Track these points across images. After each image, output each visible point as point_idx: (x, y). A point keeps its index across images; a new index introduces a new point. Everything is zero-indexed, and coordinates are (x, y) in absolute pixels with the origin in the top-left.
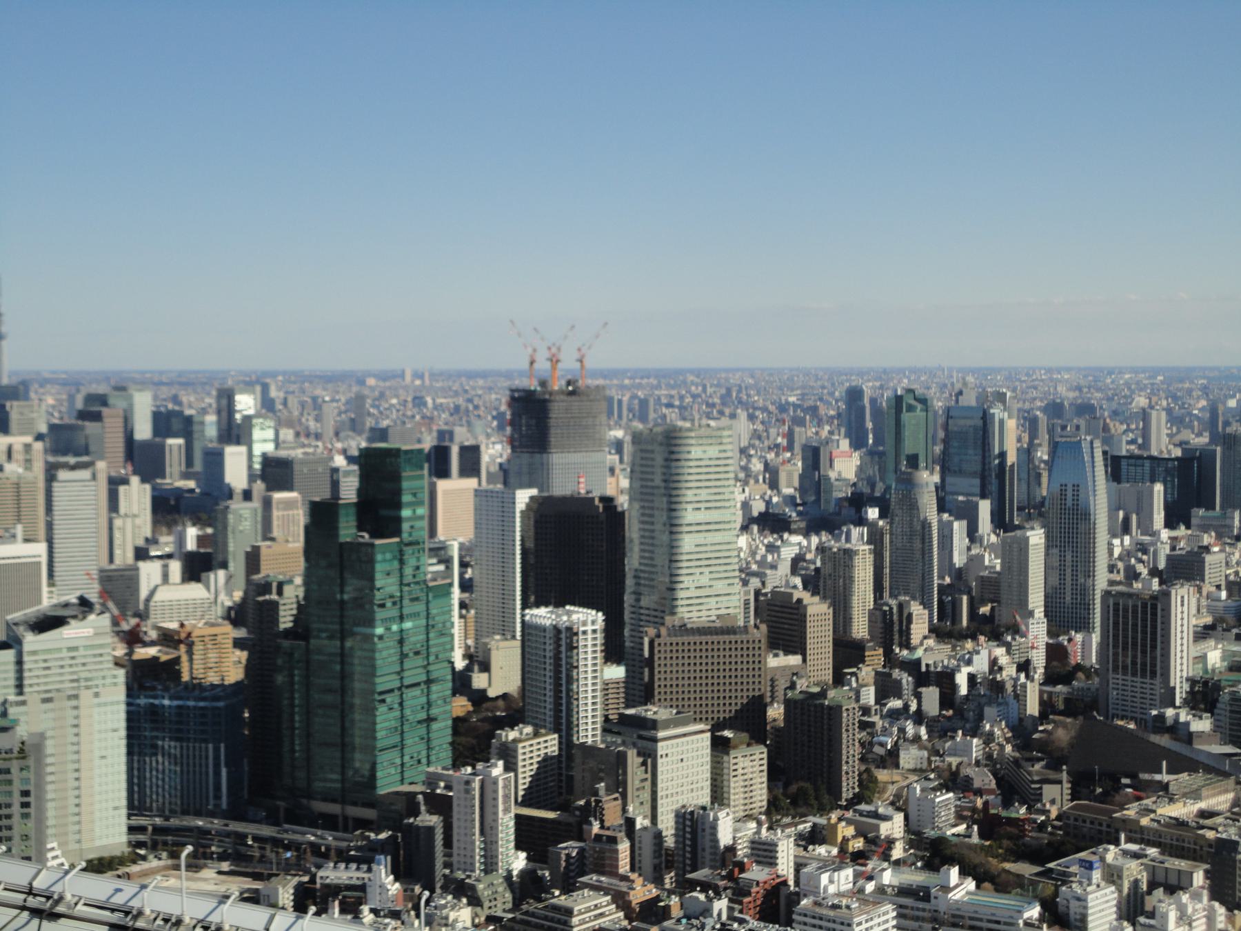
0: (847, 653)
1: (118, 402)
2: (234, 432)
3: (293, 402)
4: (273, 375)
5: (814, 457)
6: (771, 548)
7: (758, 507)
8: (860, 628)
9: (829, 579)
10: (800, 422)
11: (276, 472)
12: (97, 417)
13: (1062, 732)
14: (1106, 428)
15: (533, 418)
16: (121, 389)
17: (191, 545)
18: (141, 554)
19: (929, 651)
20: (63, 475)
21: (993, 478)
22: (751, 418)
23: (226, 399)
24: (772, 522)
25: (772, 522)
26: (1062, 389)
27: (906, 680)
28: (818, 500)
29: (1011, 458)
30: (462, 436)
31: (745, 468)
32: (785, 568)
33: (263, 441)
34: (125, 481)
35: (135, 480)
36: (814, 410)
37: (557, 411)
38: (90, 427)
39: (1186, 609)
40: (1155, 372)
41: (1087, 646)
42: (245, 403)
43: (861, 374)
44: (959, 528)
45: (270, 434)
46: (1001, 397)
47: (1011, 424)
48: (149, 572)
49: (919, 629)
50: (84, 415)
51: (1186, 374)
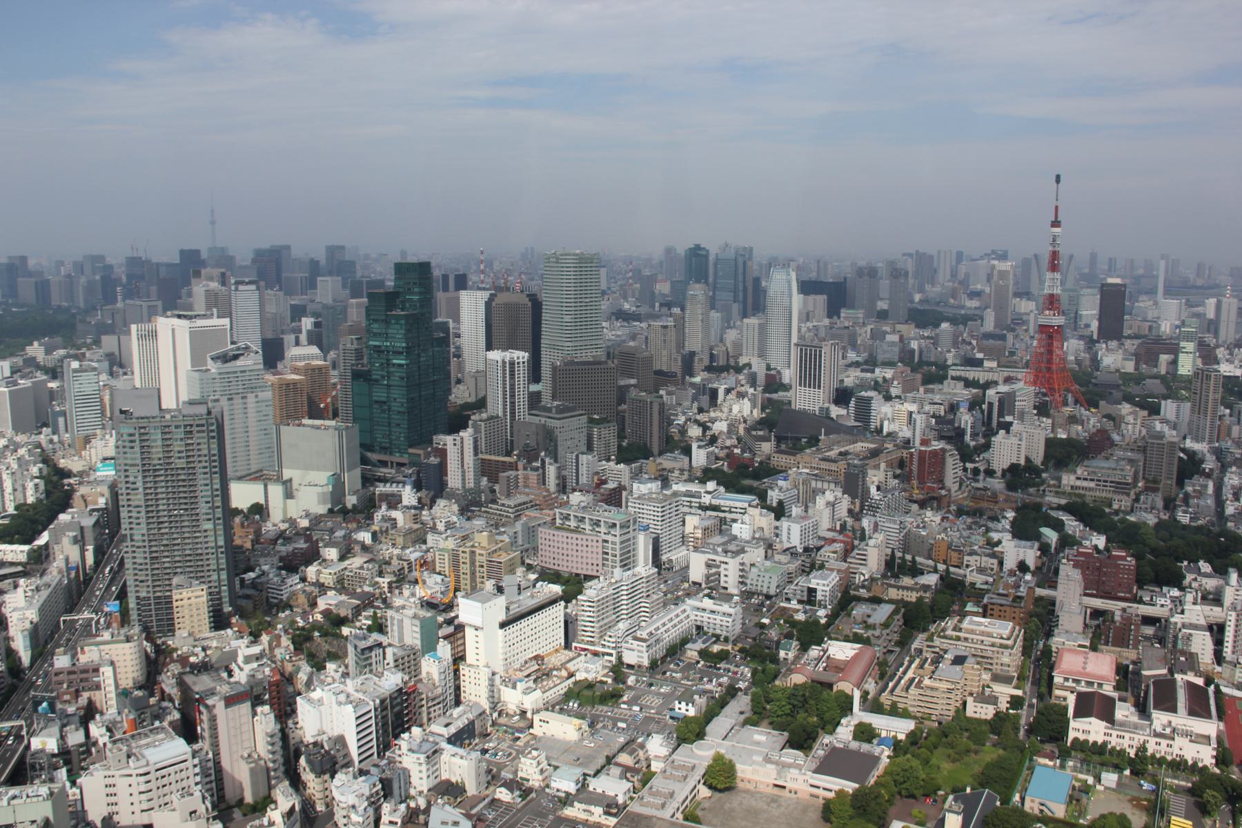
49: (697, 366)
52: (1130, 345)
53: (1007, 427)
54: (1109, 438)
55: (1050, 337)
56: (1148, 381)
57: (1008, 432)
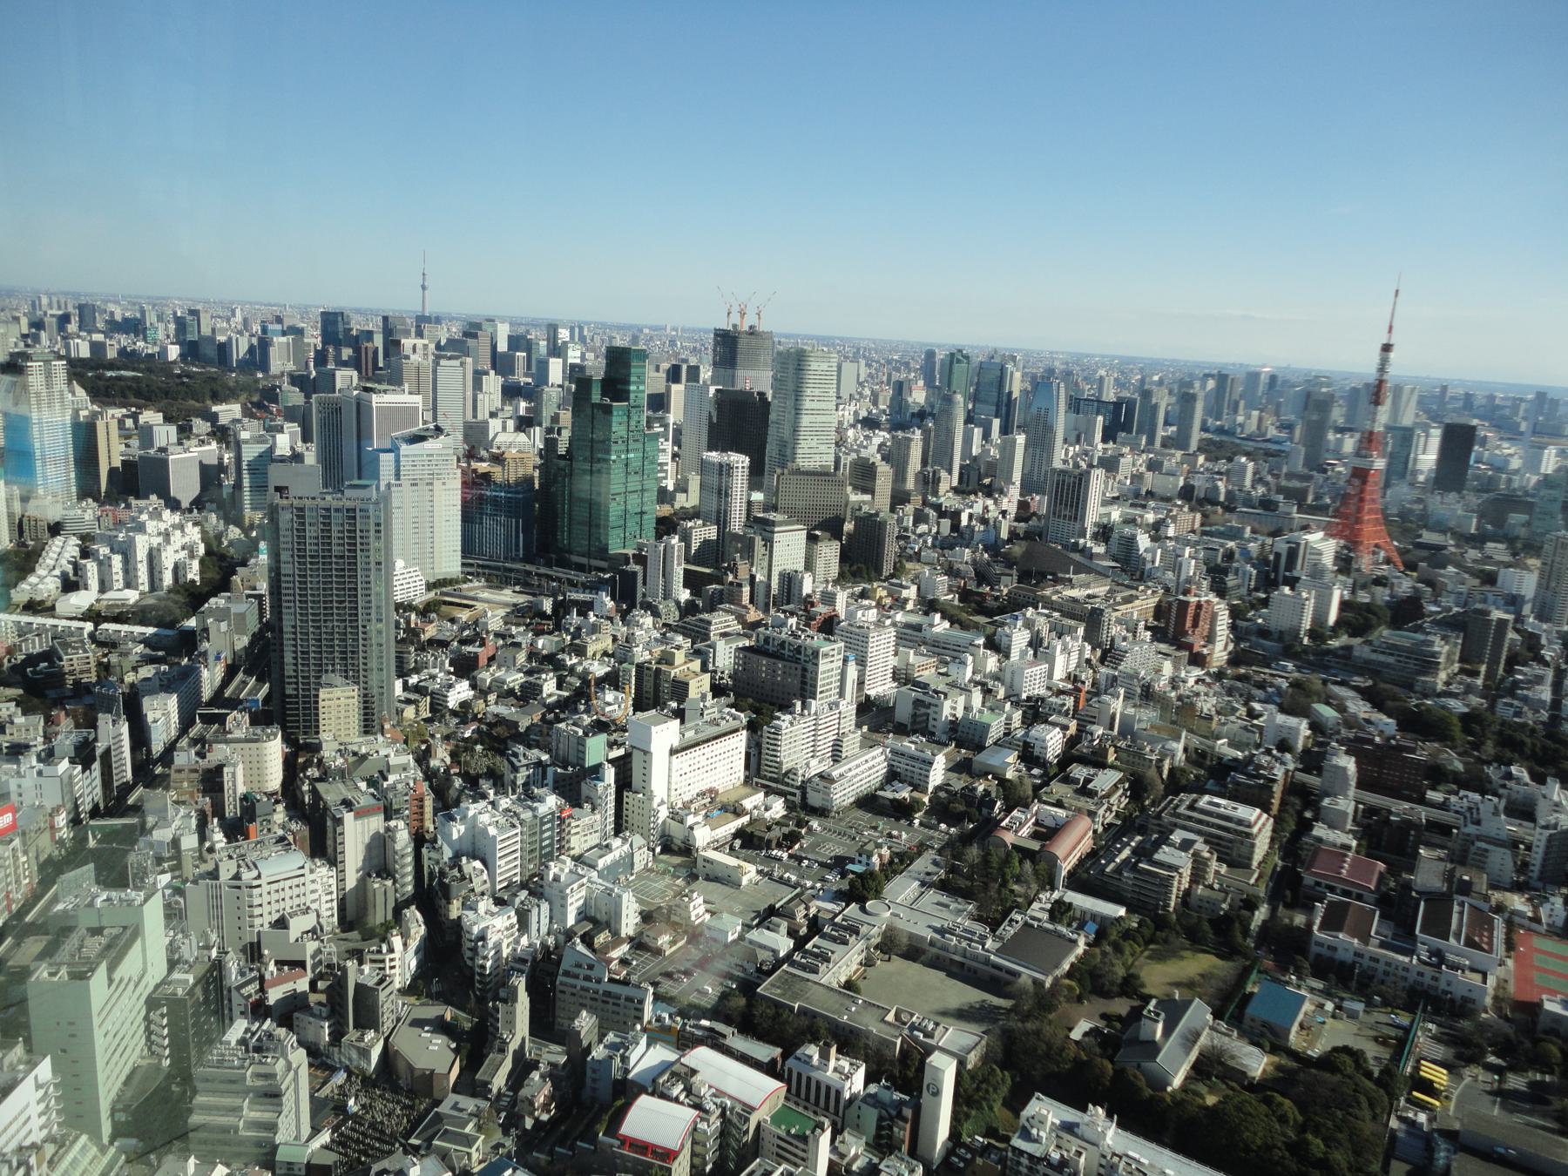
0: (899, 498)
1: (485, 325)
2: (557, 350)
3: (597, 339)
4: (588, 324)
5: (900, 388)
6: (867, 437)
7: (863, 414)
8: (910, 484)
9: (895, 456)
10: (898, 370)
11: (576, 374)
12: (475, 336)
13: (1018, 549)
14: (1077, 384)
15: (728, 346)
16: (491, 320)
17: (522, 412)
18: (493, 415)
19: (948, 500)
20: (443, 362)
21: (1005, 407)
22: (869, 366)
23: (553, 329)
24: (870, 423)
25: (870, 423)
26: (1057, 364)
27: (932, 514)
28: (899, 412)
29: (1016, 394)
30: (693, 361)
31: (860, 394)
32: (873, 449)
33: (574, 356)
34: (487, 373)
35: (492, 373)
36: (907, 364)
37: (742, 343)
38: (471, 342)
39: (1098, 485)
40: (1114, 358)
41: (1040, 503)
42: (564, 334)
43: (939, 346)
44: (977, 432)
45: (578, 354)
46: (1014, 359)
47: (1018, 375)
48: (495, 425)
49: (944, 487)
50: (466, 334)
51: (1132, 361)
52: (1474, 500)
53: (1293, 582)
54: (1421, 607)
55: (1364, 482)
56: (1490, 545)
57: (1292, 589)
